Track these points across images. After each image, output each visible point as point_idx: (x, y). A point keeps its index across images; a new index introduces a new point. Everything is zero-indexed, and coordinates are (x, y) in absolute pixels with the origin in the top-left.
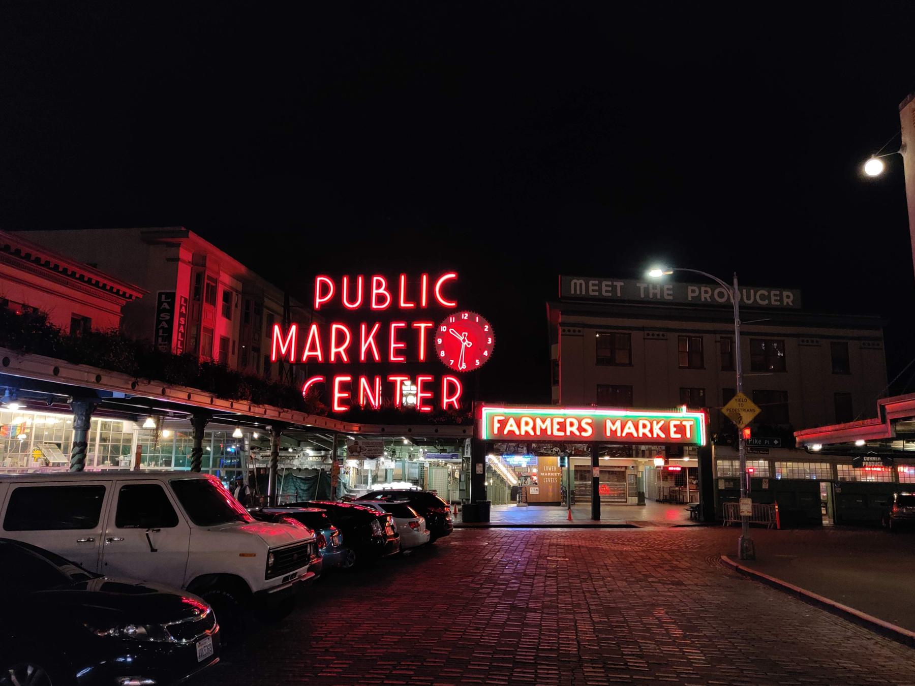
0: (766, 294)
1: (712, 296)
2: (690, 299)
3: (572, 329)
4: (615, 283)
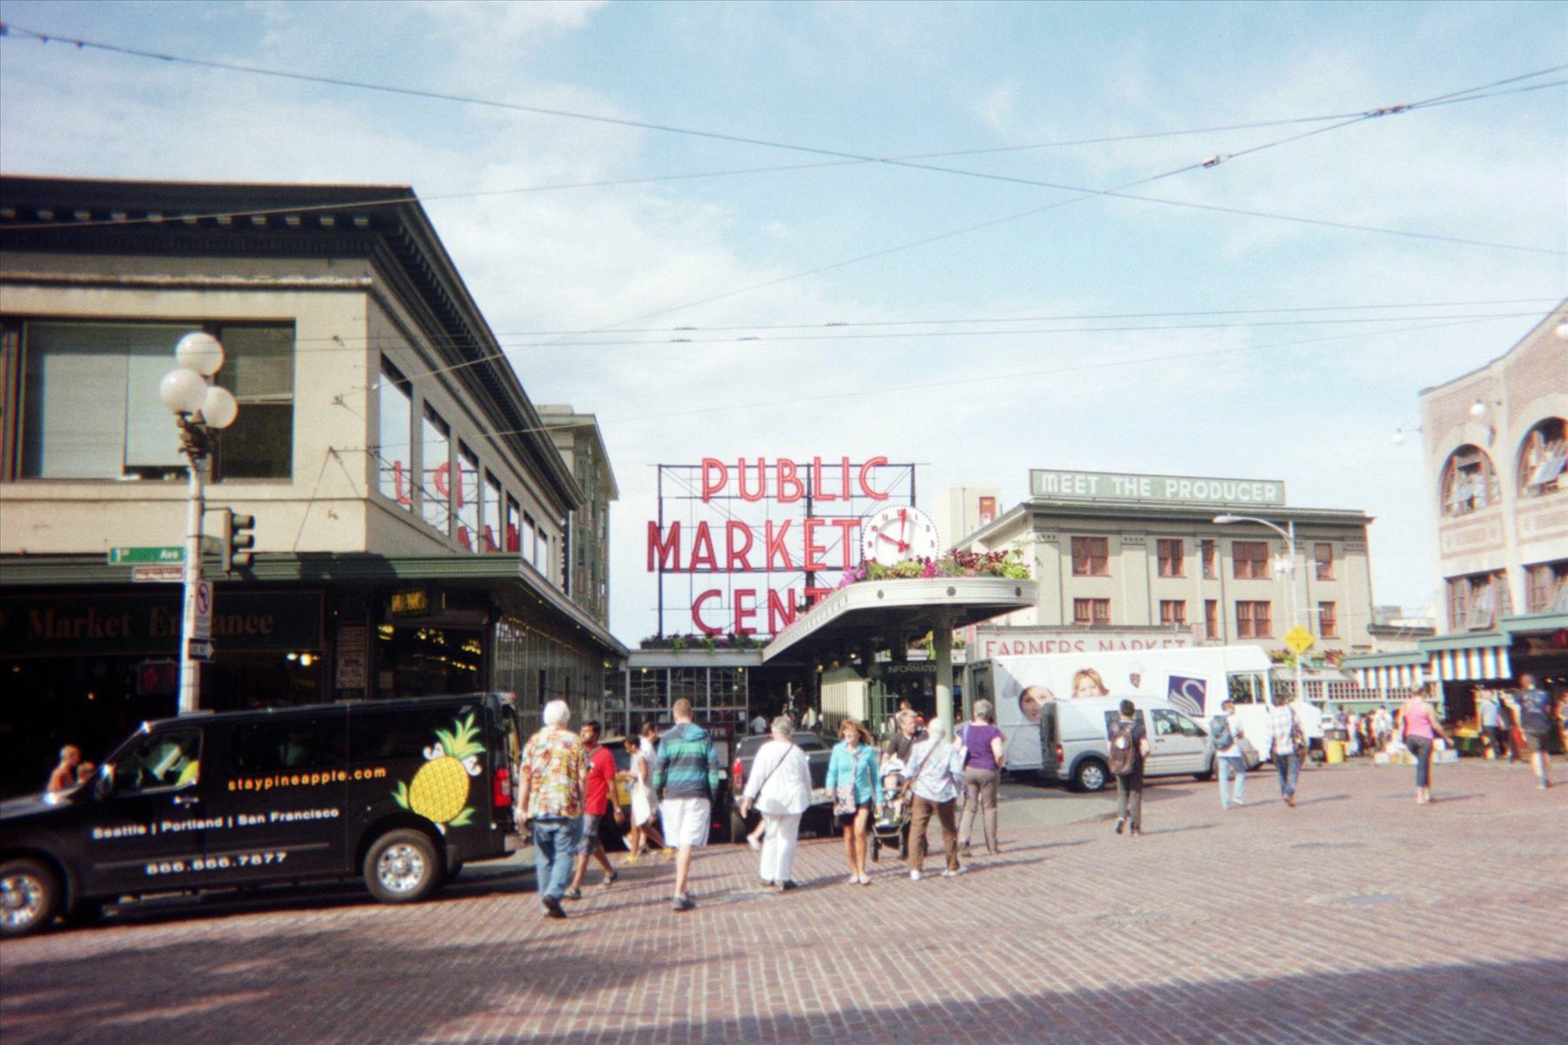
1: (1191, 493)
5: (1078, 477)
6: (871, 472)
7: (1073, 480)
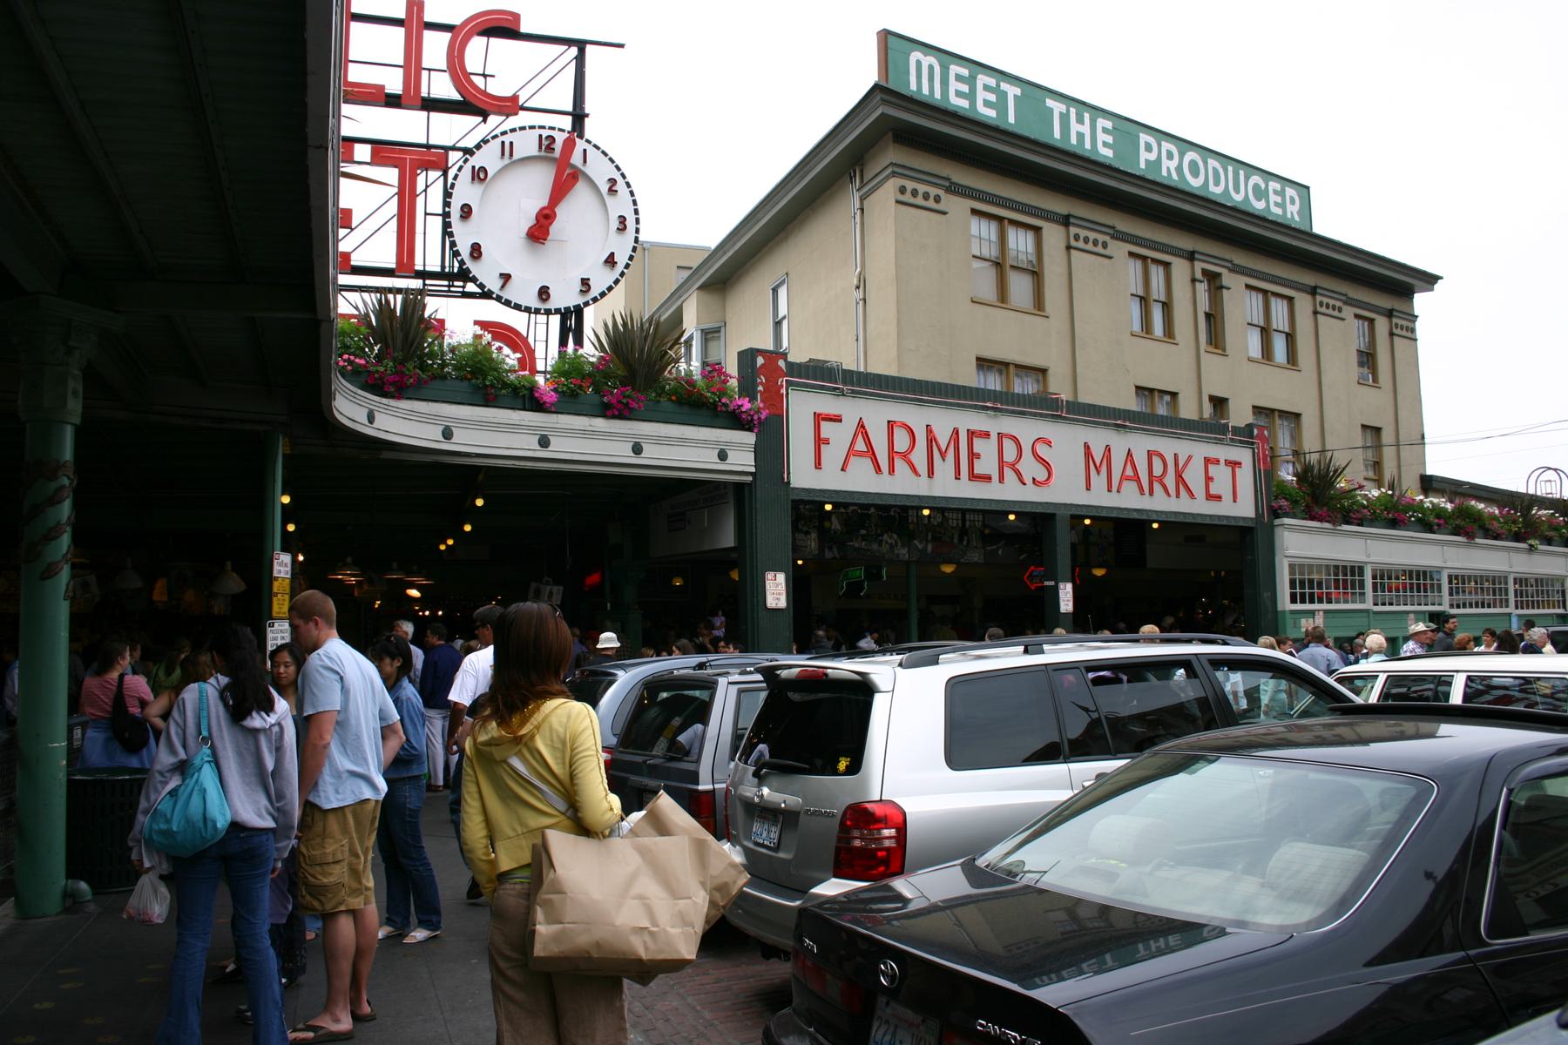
0: (1263, 186)
1: (1179, 169)
2: (1142, 166)
3: (922, 188)
4: (1004, 86)
5: (983, 79)
6: (476, 49)
7: (971, 81)
